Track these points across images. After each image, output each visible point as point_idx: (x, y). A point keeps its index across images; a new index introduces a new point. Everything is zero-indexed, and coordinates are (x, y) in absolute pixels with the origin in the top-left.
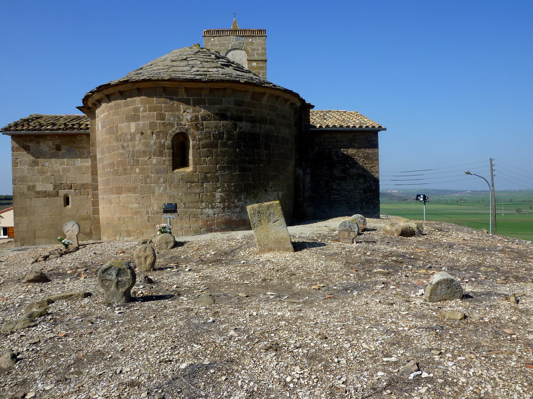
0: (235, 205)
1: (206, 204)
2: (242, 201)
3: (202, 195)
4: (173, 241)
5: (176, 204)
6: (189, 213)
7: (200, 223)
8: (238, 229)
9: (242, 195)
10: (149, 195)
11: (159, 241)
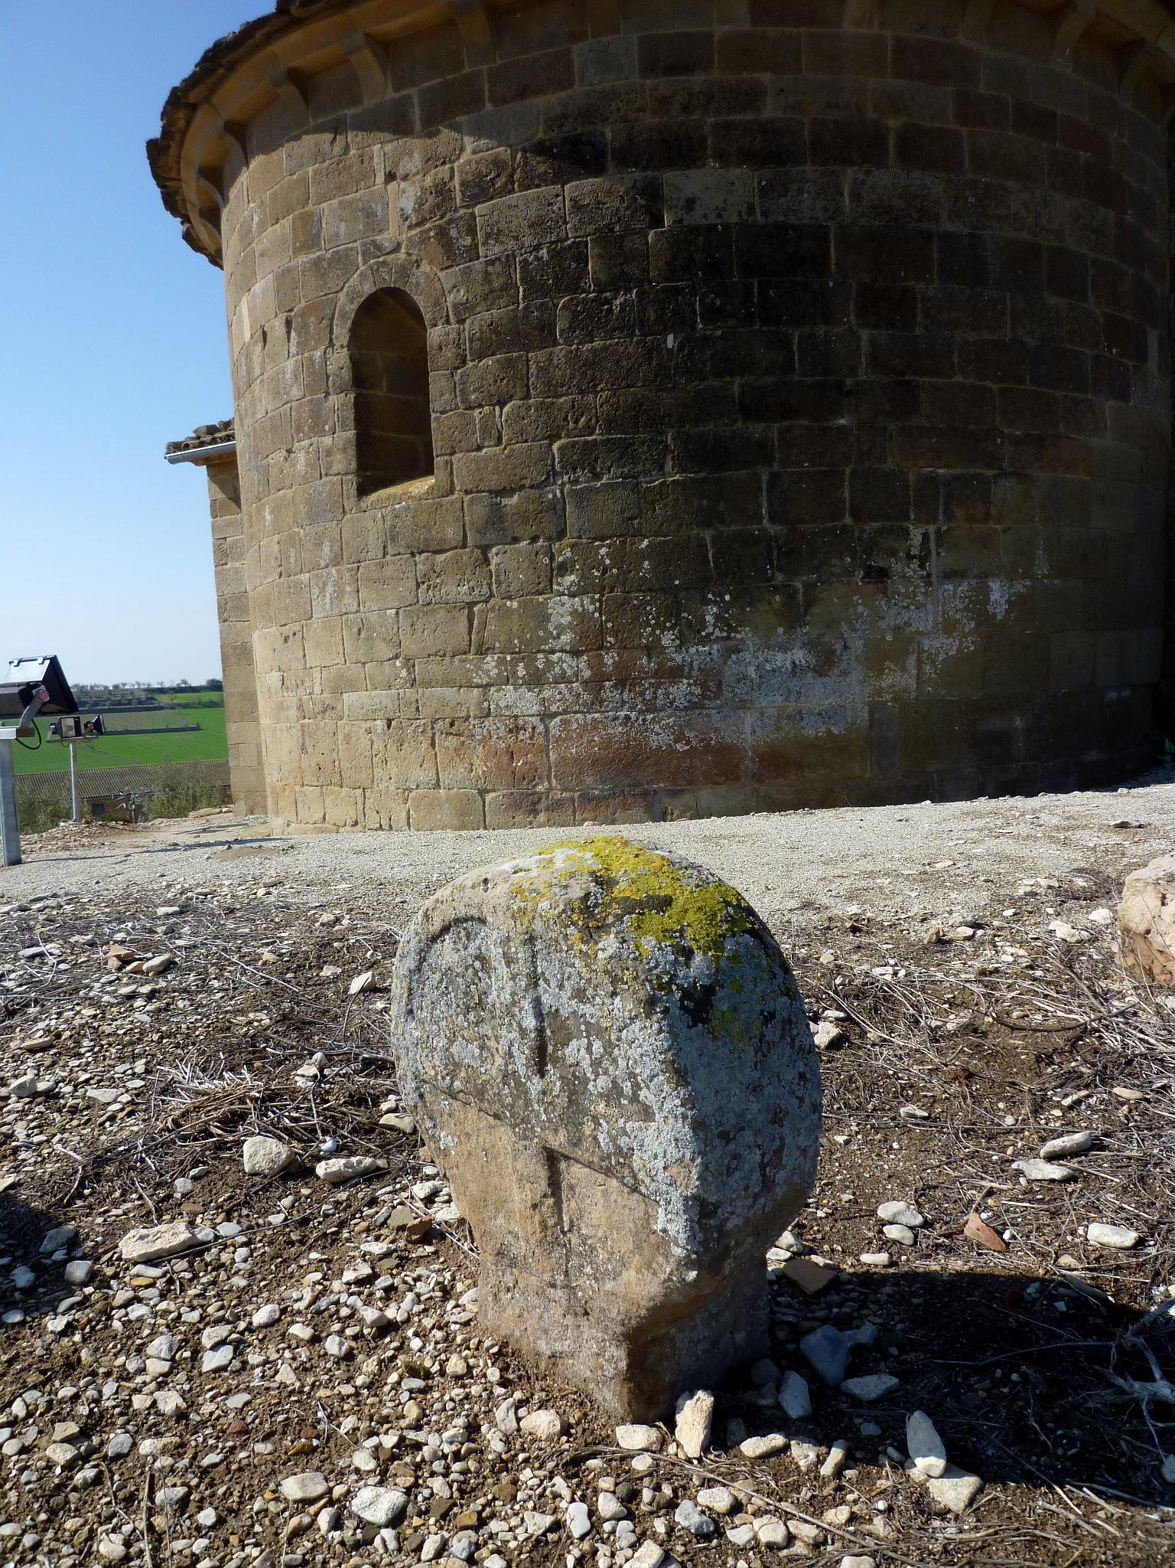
0: (661, 665)
1: (501, 662)
2: (706, 640)
7: (477, 762)
9: (708, 602)
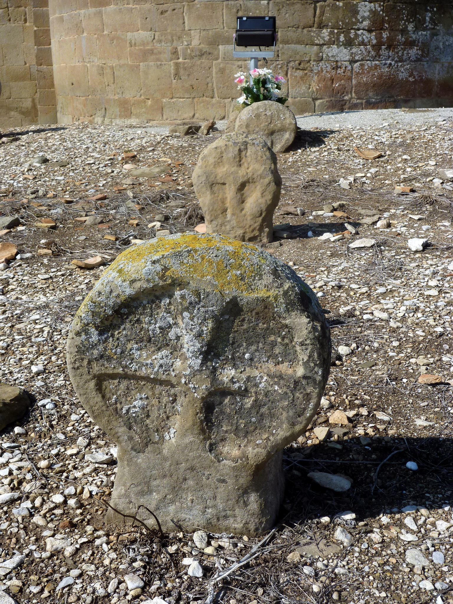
0: (407, 39)
1: (331, 33)
2: (425, 29)
3: (322, 7)
4: (292, 127)
5: (273, 19)
6: (285, 57)
7: (313, 84)
8: (411, 103)
9: (427, 11)
10: (179, 5)
11: (247, 126)
